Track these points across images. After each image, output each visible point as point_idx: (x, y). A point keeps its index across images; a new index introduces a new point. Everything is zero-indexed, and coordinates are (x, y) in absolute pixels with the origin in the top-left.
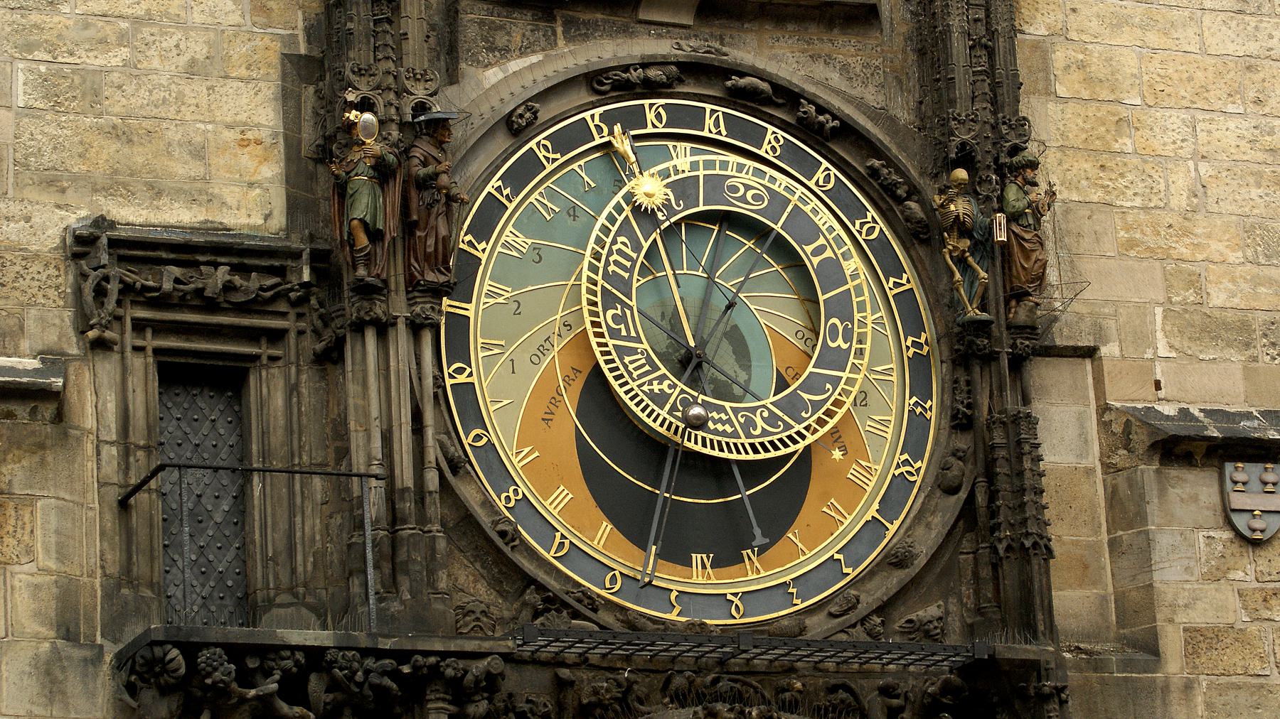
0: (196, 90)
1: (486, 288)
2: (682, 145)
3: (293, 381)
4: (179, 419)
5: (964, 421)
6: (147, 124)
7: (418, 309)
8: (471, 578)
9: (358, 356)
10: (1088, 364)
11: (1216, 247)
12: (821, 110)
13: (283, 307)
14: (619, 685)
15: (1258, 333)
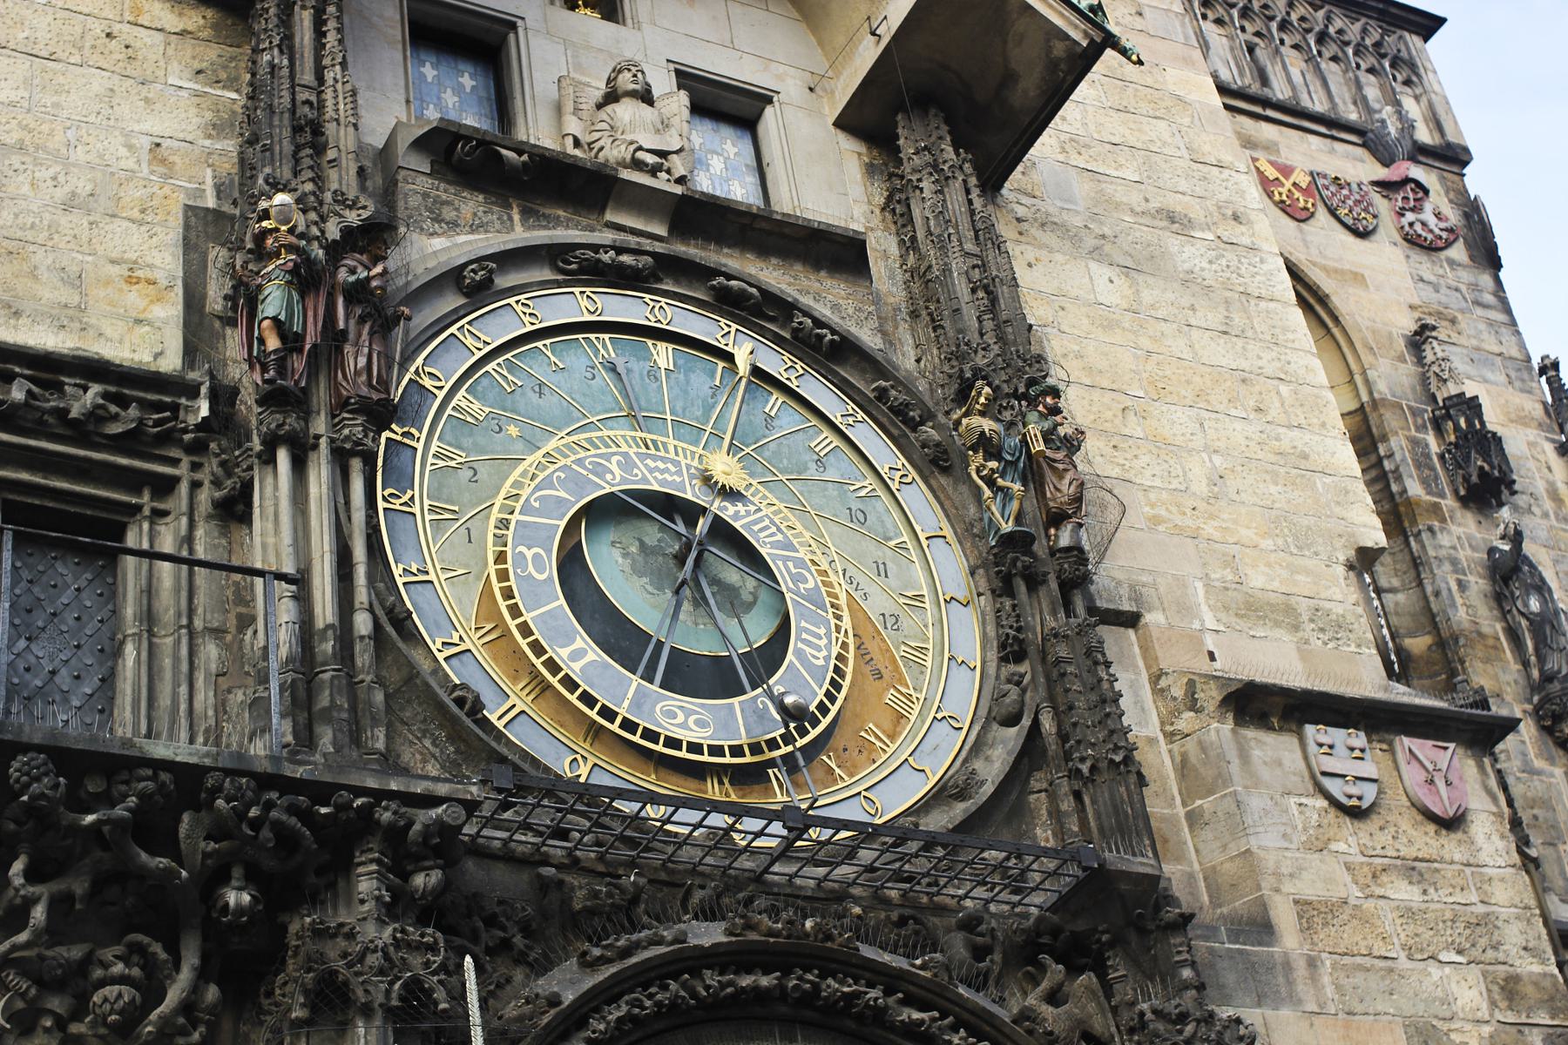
0: (75, 222)
1: (433, 449)
2: (662, 346)
3: (183, 532)
4: (30, 582)
5: (1016, 648)
6: (11, 245)
7: (346, 432)
8: (418, 757)
9: (269, 490)
10: (1131, 632)
11: (1247, 534)
12: (818, 323)
13: (175, 453)
14: (623, 891)
15: (1305, 618)
